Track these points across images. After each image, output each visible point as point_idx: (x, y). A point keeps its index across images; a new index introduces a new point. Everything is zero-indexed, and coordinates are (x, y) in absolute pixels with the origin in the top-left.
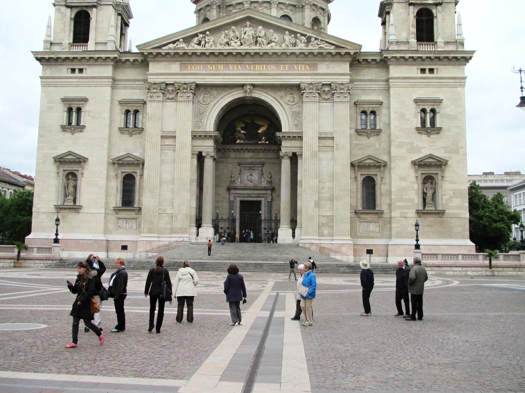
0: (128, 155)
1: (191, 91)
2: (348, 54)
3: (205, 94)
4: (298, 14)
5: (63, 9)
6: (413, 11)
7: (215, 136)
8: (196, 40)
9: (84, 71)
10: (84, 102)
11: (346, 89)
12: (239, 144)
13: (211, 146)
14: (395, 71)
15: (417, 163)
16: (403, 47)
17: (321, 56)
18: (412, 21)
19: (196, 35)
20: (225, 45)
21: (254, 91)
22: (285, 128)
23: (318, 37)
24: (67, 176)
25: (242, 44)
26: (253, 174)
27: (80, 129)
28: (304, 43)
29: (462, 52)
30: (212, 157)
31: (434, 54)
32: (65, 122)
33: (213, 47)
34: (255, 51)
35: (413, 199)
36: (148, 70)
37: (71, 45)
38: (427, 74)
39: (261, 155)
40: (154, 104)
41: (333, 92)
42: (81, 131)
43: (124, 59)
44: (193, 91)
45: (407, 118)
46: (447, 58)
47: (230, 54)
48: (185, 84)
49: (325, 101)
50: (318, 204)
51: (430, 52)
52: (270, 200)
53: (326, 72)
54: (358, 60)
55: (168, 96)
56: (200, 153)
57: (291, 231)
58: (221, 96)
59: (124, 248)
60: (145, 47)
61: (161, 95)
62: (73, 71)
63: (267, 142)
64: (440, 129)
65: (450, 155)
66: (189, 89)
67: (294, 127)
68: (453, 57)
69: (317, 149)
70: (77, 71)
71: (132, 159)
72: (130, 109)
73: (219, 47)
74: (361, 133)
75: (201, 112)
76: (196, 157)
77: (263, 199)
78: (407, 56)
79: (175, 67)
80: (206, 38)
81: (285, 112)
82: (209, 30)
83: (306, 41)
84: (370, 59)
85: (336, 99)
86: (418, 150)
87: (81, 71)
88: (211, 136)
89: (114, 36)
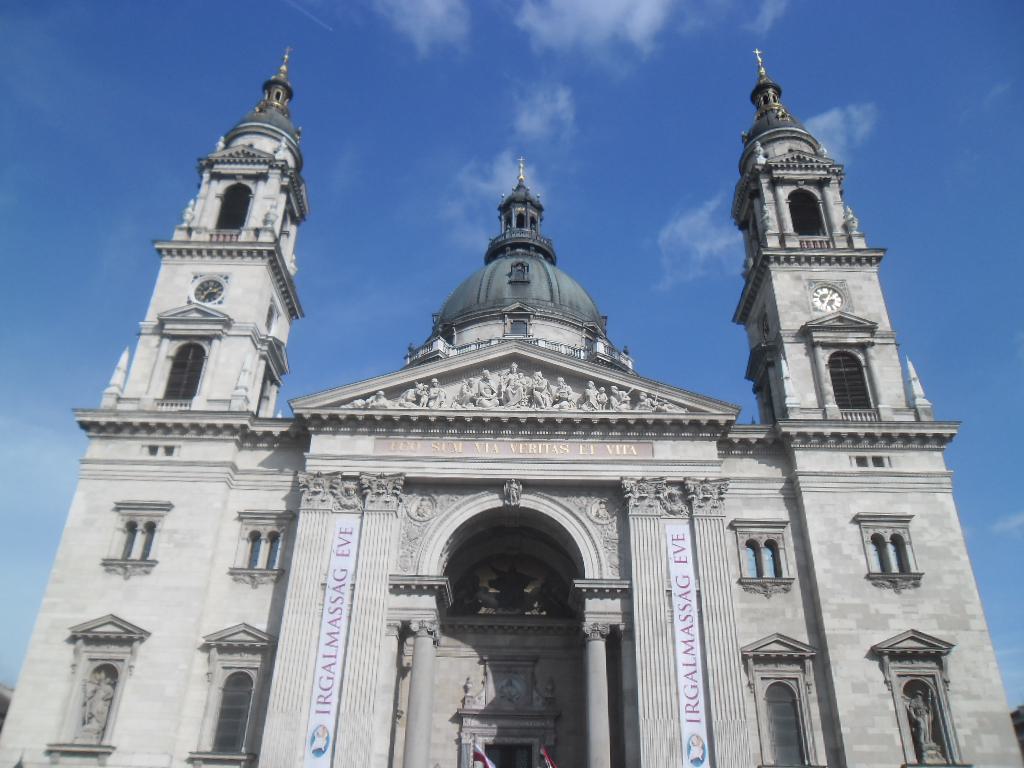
0: (247, 629)
1: (395, 491)
2: (713, 424)
3: (422, 500)
5: (155, 340)
6: (824, 356)
7: (441, 587)
8: (411, 392)
9: (176, 451)
10: (164, 512)
12: (485, 615)
13: (430, 610)
15: (886, 651)
17: (660, 429)
19: (412, 385)
21: (523, 496)
22: (591, 572)
23: (653, 392)
25: (501, 404)
26: (515, 683)
27: (144, 568)
28: (625, 402)
30: (430, 633)
31: (880, 427)
33: (445, 406)
34: (530, 415)
35: (891, 737)
36: (308, 450)
37: (160, 402)
38: (871, 468)
39: (531, 641)
40: (312, 516)
41: (690, 497)
42: (147, 573)
44: (398, 492)
45: (846, 551)
46: (906, 439)
47: (478, 422)
48: (382, 477)
49: (672, 516)
52: (552, 743)
53: (671, 458)
54: (731, 439)
55: (345, 501)
58: (456, 505)
60: (310, 403)
61: (331, 498)
62: (153, 450)
63: (544, 613)
64: (918, 577)
65: (953, 633)
66: (390, 486)
67: (610, 570)
68: (918, 434)
70: (161, 451)
71: (250, 638)
72: (260, 529)
73: (459, 408)
74: (752, 586)
75: (415, 536)
76: (396, 633)
77: (536, 741)
79: (364, 444)
80: (431, 390)
81: (591, 538)
82: (436, 376)
83: (629, 398)
84: (754, 438)
85: (697, 512)
86: (882, 621)
87: (169, 450)
88: (431, 587)
89: (246, 389)
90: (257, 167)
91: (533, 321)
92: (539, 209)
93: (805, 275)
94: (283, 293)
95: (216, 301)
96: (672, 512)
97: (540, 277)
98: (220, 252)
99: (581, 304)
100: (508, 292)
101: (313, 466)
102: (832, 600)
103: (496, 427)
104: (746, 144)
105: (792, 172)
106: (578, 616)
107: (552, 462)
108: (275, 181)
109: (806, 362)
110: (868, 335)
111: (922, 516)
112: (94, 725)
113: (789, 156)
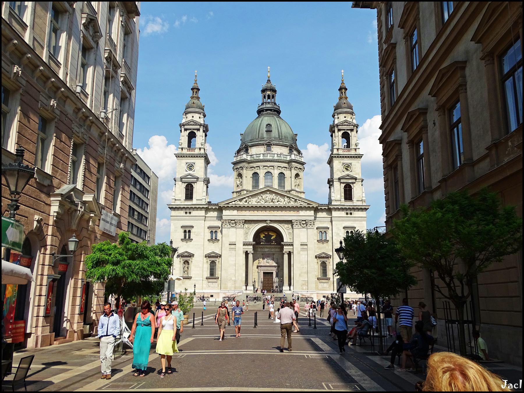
0: (213, 252)
4: (288, 171)
6: (343, 185)
8: (244, 200)
11: (312, 222)
12: (262, 245)
14: (335, 214)
16: (338, 203)
18: (343, 190)
19: (245, 198)
20: (258, 203)
24: (184, 263)
29: (364, 206)
32: (183, 238)
38: (349, 215)
39: (273, 250)
40: (225, 229)
43: (210, 207)
45: (340, 235)
48: (239, 220)
50: (300, 275)
51: (350, 206)
55: (232, 225)
56: (247, 251)
57: (289, 287)
59: (212, 296)
62: (186, 213)
66: (241, 222)
69: (300, 250)
70: (188, 213)
72: (213, 230)
73: (256, 204)
78: (340, 207)
79: (235, 212)
85: (308, 227)
87: (190, 213)
90: (197, 126)
91: (274, 146)
92: (274, 91)
93: (342, 161)
94: (207, 162)
95: (193, 171)
96: (303, 227)
97: (275, 128)
98: (192, 156)
99: (288, 135)
100: (265, 135)
101: (224, 218)
102: (335, 245)
103: (264, 208)
104: (335, 110)
105: (344, 127)
106: (282, 249)
107: (276, 216)
108: (201, 130)
109: (339, 187)
110: (355, 180)
111: (358, 227)
112: (186, 273)
113: (343, 122)
